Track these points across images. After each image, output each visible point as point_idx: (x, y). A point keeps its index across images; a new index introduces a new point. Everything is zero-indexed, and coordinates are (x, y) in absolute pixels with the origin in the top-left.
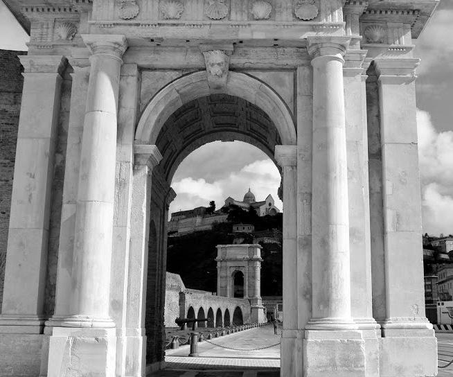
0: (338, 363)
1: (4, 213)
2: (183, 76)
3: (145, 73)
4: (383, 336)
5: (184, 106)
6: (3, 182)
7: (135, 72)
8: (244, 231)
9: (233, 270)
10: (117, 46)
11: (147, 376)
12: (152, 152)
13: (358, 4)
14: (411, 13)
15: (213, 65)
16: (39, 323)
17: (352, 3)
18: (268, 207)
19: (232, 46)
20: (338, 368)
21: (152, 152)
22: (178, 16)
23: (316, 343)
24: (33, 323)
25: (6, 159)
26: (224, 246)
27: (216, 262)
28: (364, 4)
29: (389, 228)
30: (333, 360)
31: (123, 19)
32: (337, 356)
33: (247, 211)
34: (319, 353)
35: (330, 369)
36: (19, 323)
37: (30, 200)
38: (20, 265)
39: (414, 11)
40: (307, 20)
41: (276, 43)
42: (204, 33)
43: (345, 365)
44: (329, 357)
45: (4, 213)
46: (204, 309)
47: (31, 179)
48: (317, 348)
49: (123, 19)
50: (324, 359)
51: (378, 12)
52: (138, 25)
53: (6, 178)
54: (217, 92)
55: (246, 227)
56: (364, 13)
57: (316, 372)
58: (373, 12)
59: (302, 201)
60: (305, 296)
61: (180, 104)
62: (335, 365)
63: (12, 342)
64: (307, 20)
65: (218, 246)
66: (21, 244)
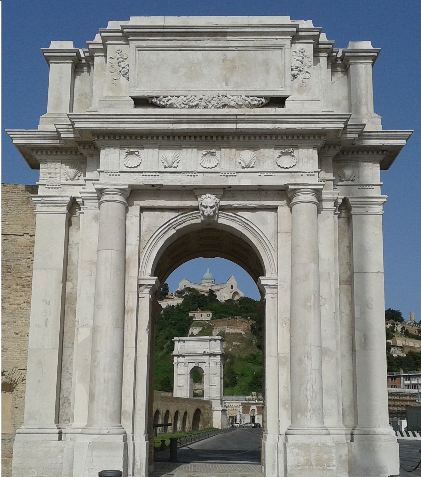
0: (314, 463)
1: (17, 334)
2: (180, 215)
3: (145, 214)
4: (352, 440)
5: (178, 238)
6: (16, 306)
7: (138, 212)
8: (201, 319)
9: (192, 366)
10: (123, 192)
11: (149, 475)
12: (154, 283)
13: (332, 148)
14: (380, 153)
15: (206, 207)
16: (57, 431)
17: (327, 148)
18: (231, 290)
19: (222, 190)
20: (314, 467)
21: (154, 283)
22: (175, 165)
23: (295, 445)
24: (53, 431)
25: (17, 284)
26: (181, 338)
27: (173, 357)
28: (337, 148)
29: (357, 348)
30: (308, 460)
31: (127, 167)
32: (313, 456)
33: (206, 294)
34: (297, 454)
35: (306, 467)
36: (40, 431)
37: (46, 325)
38: (39, 381)
39: (383, 151)
40: (287, 168)
41: (260, 187)
42: (198, 181)
43: (318, 465)
44: (306, 458)
45: (17, 334)
46: (161, 412)
47: (47, 305)
48: (296, 450)
49: (127, 167)
50: (302, 459)
51: (350, 153)
52: (141, 172)
53: (17, 302)
54: (209, 227)
55: (205, 314)
56: (338, 154)
57: (295, 470)
58: (345, 153)
59: (282, 325)
60: (285, 406)
61: (176, 238)
62: (311, 465)
63: (35, 448)
64: (287, 168)
65: (176, 339)
66: (40, 363)
